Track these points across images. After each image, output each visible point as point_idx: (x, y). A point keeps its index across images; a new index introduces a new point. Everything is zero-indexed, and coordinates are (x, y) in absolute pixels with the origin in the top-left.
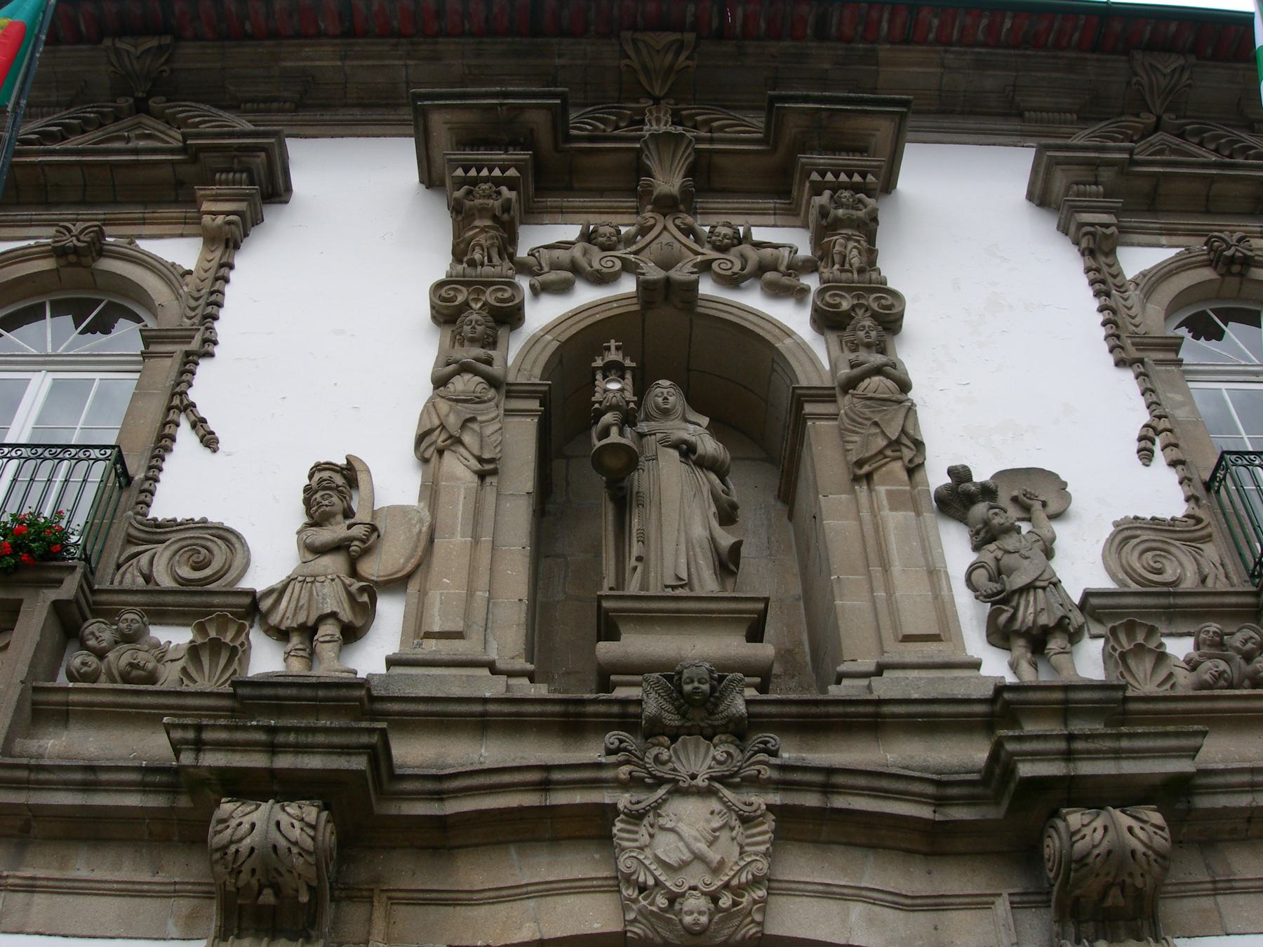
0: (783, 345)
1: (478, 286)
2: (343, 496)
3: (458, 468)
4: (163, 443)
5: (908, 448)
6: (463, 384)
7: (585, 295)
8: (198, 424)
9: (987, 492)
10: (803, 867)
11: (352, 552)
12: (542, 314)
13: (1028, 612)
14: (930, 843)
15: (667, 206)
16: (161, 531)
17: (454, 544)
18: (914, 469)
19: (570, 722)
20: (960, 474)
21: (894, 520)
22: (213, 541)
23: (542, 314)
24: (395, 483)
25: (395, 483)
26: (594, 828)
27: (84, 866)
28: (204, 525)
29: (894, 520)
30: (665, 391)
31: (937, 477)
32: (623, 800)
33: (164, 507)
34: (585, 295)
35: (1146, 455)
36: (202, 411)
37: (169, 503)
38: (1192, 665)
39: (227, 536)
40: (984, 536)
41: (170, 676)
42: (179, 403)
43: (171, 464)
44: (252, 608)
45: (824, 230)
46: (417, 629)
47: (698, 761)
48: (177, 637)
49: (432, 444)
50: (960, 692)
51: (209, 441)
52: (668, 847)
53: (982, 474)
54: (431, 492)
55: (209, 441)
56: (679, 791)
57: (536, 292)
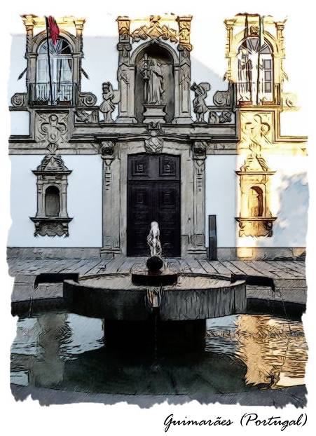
1: (124, 44)
2: (108, 88)
4: (80, 76)
6: (124, 67)
7: (142, 42)
8: (85, 74)
10: (166, 144)
11: (110, 99)
12: (135, 46)
20: (195, 84)
22: (91, 96)
24: (115, 85)
25: (115, 85)
26: (144, 140)
28: (89, 93)
29: (185, 92)
30: (155, 61)
31: (192, 84)
32: (146, 137)
33: (84, 89)
36: (85, 71)
37: (84, 89)
38: (220, 117)
40: (196, 95)
43: (82, 81)
44: (98, 108)
46: (120, 111)
47: (154, 133)
51: (86, 76)
52: (151, 144)
53: (198, 84)
55: (86, 76)
56: (152, 137)
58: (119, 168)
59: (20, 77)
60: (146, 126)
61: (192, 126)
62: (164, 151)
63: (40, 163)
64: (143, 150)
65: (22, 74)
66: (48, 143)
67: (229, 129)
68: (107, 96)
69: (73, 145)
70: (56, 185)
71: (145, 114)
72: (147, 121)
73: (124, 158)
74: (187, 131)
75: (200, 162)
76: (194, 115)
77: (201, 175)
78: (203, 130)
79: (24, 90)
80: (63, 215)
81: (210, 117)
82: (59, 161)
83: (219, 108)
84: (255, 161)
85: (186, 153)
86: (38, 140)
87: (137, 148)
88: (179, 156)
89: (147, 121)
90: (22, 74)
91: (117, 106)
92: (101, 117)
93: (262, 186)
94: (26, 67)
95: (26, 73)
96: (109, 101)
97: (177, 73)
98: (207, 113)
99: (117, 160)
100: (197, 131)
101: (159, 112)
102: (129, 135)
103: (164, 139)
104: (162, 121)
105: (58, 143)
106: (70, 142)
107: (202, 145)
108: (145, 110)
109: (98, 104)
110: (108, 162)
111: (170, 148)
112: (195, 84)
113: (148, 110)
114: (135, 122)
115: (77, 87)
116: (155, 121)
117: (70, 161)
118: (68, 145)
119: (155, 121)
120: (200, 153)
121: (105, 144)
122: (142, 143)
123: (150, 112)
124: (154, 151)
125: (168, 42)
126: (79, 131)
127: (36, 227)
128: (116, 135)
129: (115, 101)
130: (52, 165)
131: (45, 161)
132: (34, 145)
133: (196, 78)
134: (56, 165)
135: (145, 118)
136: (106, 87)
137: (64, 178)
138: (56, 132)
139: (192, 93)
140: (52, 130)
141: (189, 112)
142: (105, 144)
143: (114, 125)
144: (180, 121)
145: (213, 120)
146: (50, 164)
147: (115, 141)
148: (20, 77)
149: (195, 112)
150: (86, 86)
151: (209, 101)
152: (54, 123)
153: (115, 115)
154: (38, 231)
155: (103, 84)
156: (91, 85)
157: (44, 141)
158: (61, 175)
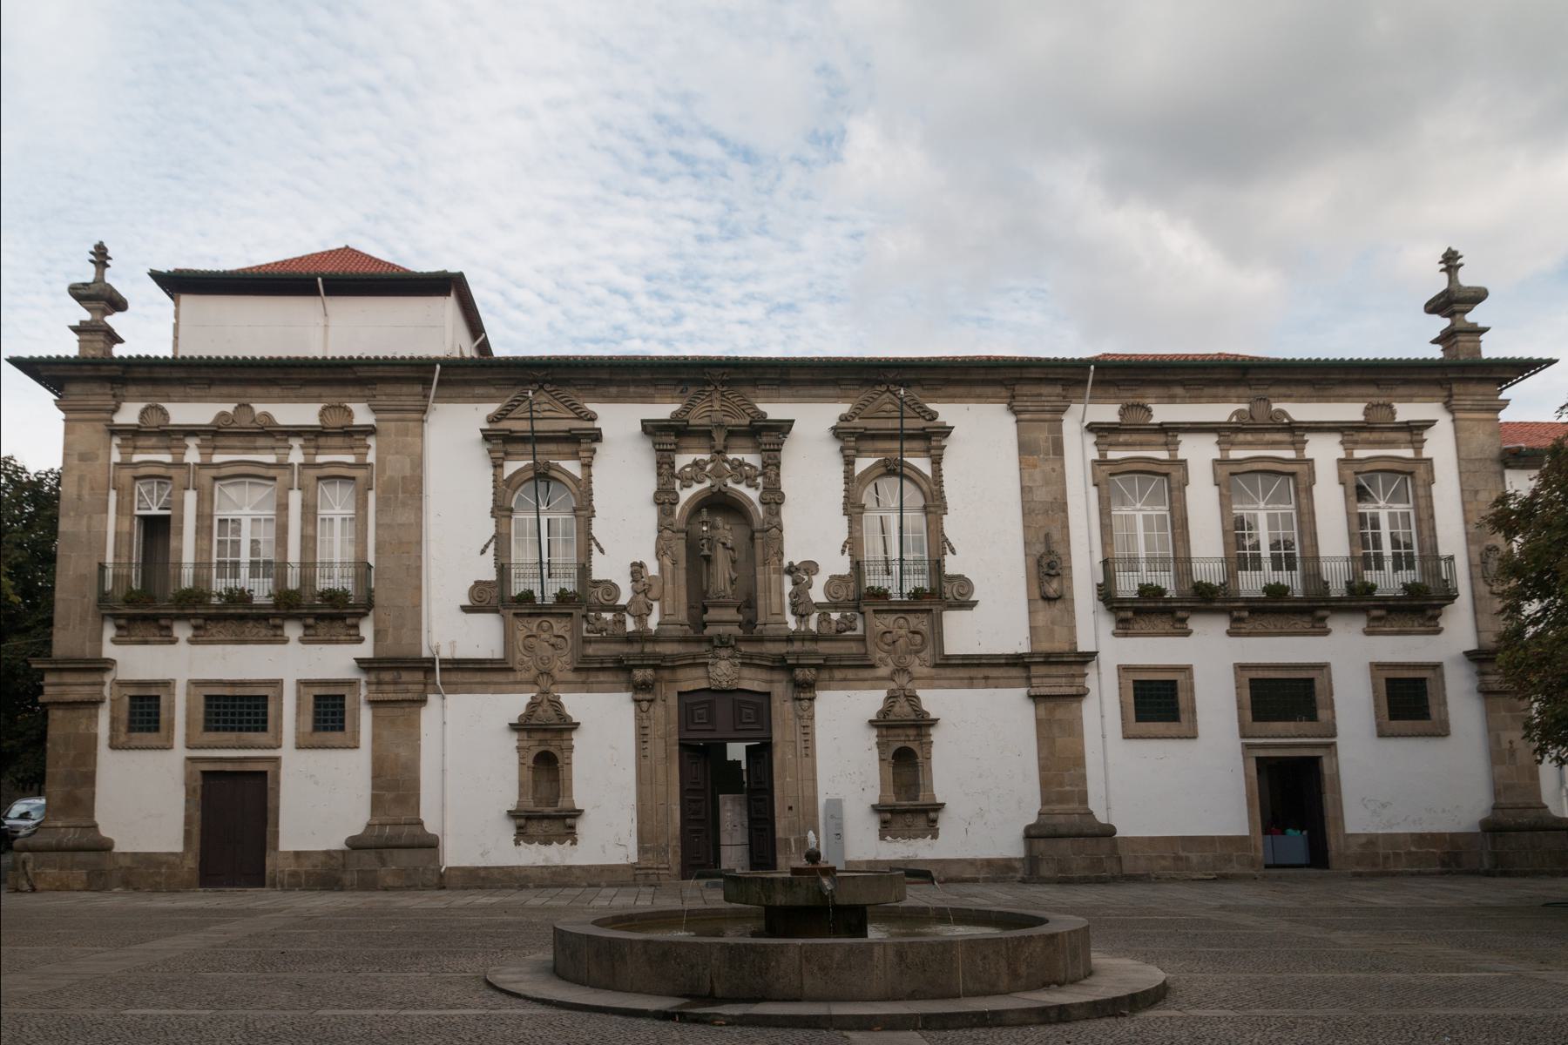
0: (751, 508)
3: (667, 561)
5: (780, 553)
6: (667, 533)
7: (697, 488)
8: (598, 545)
9: (797, 569)
10: (746, 672)
13: (800, 610)
14: (772, 668)
15: (718, 452)
16: (597, 583)
17: (669, 586)
18: (780, 560)
19: (699, 641)
20: (791, 564)
21: (774, 577)
22: (611, 588)
23: (685, 495)
24: (653, 568)
25: (653, 568)
27: (602, 677)
29: (774, 577)
31: (786, 563)
33: (596, 576)
34: (697, 488)
35: (843, 552)
37: (596, 576)
38: (838, 622)
39: (614, 585)
40: (795, 583)
41: (610, 628)
42: (590, 537)
43: (594, 558)
44: (624, 608)
45: (765, 465)
46: (663, 613)
48: (608, 616)
49: (660, 553)
50: (782, 633)
51: (602, 551)
54: (662, 569)
55: (602, 551)
57: (683, 486)
58: (666, 711)
59: (483, 552)
60: (710, 640)
61: (790, 639)
62: (746, 685)
63: (522, 710)
64: (704, 685)
65: (486, 546)
66: (534, 672)
67: (853, 644)
68: (640, 586)
69: (582, 677)
70: (552, 749)
71: (705, 617)
72: (710, 631)
73: (673, 700)
74: (781, 648)
75: (806, 704)
76: (792, 623)
77: (807, 732)
78: (809, 646)
79: (490, 575)
80: (563, 804)
81: (819, 623)
82: (556, 705)
83: (835, 606)
84: (902, 699)
85: (780, 688)
86: (518, 667)
87: (692, 680)
88: (768, 694)
89: (710, 631)
90: (486, 546)
91: (656, 605)
92: (631, 625)
93: (913, 745)
94: (493, 532)
95: (492, 546)
96: (641, 596)
97: (758, 542)
98: (816, 615)
99: (659, 701)
100: (797, 646)
101: (730, 614)
102: (684, 657)
103: (743, 664)
104: (736, 630)
105: (556, 672)
106: (576, 670)
107: (809, 674)
108: (705, 610)
109: (624, 599)
110: (645, 705)
111: (752, 681)
112: (791, 564)
113: (711, 611)
114: (691, 633)
115: (584, 570)
116: (721, 630)
117: (575, 703)
118: (571, 676)
119: (721, 630)
120: (804, 690)
121: (639, 675)
122: (700, 672)
123: (713, 614)
124: (724, 685)
125: (742, 488)
126: (590, 650)
127: (519, 828)
128: (655, 656)
129: (654, 593)
130: (545, 714)
131: (533, 705)
132: (511, 677)
133: (793, 554)
134: (551, 713)
135: (705, 625)
136: (637, 569)
137: (566, 736)
138: (549, 651)
139: (787, 580)
140: (545, 650)
141: (782, 613)
142: (639, 675)
143: (655, 639)
144: (770, 630)
145: (824, 631)
146: (540, 710)
147: (656, 667)
148: (483, 552)
149: (794, 613)
150: (601, 569)
151: (817, 594)
152: (545, 636)
153: (653, 622)
154: (522, 835)
155: (633, 564)
156: (610, 567)
157: (528, 670)
158: (561, 730)
